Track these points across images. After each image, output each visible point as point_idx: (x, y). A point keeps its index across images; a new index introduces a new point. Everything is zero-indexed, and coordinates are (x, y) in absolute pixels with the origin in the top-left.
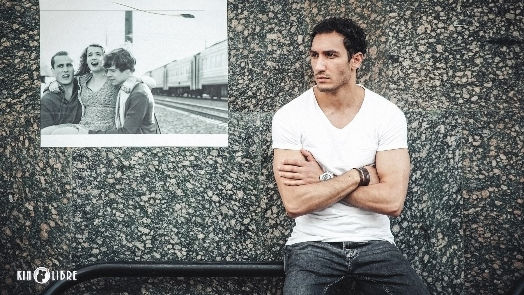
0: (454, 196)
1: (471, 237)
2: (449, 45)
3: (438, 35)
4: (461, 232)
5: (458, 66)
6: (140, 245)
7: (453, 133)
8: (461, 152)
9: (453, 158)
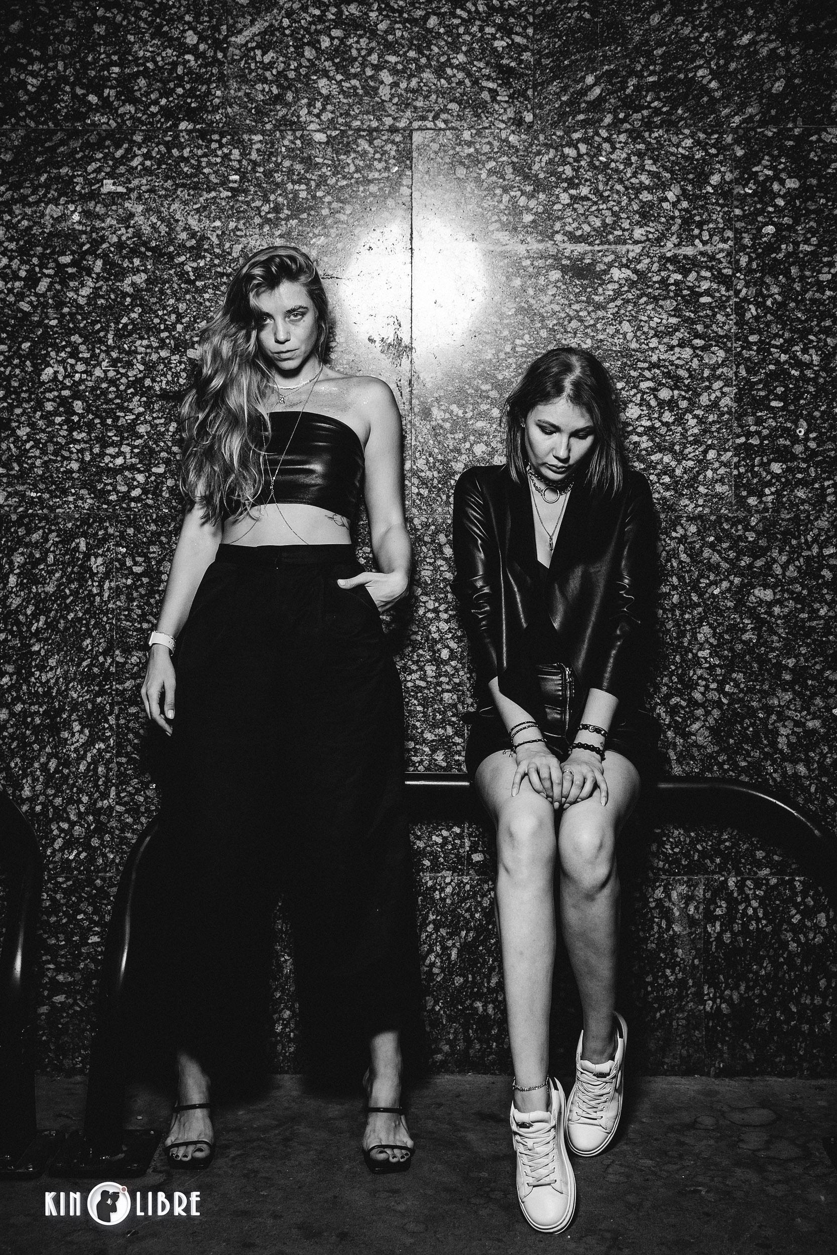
0: (101, 659)
1: (128, 728)
2: (94, 401)
3: (77, 384)
4: (112, 720)
5: (110, 437)
7: (100, 552)
8: (113, 584)
9: (100, 594)
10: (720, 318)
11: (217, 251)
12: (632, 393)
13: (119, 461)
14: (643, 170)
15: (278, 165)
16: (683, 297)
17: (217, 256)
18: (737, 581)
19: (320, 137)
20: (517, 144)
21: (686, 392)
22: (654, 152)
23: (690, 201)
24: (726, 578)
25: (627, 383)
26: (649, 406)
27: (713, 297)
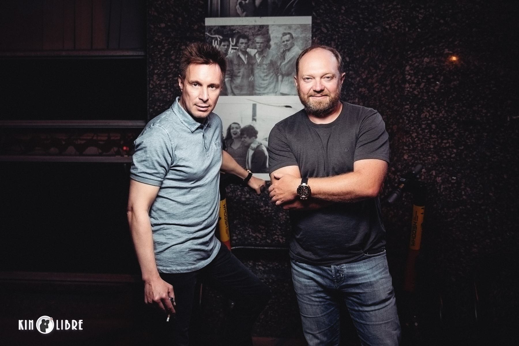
6: (260, 236)
9: (440, 190)
13: (448, 145)
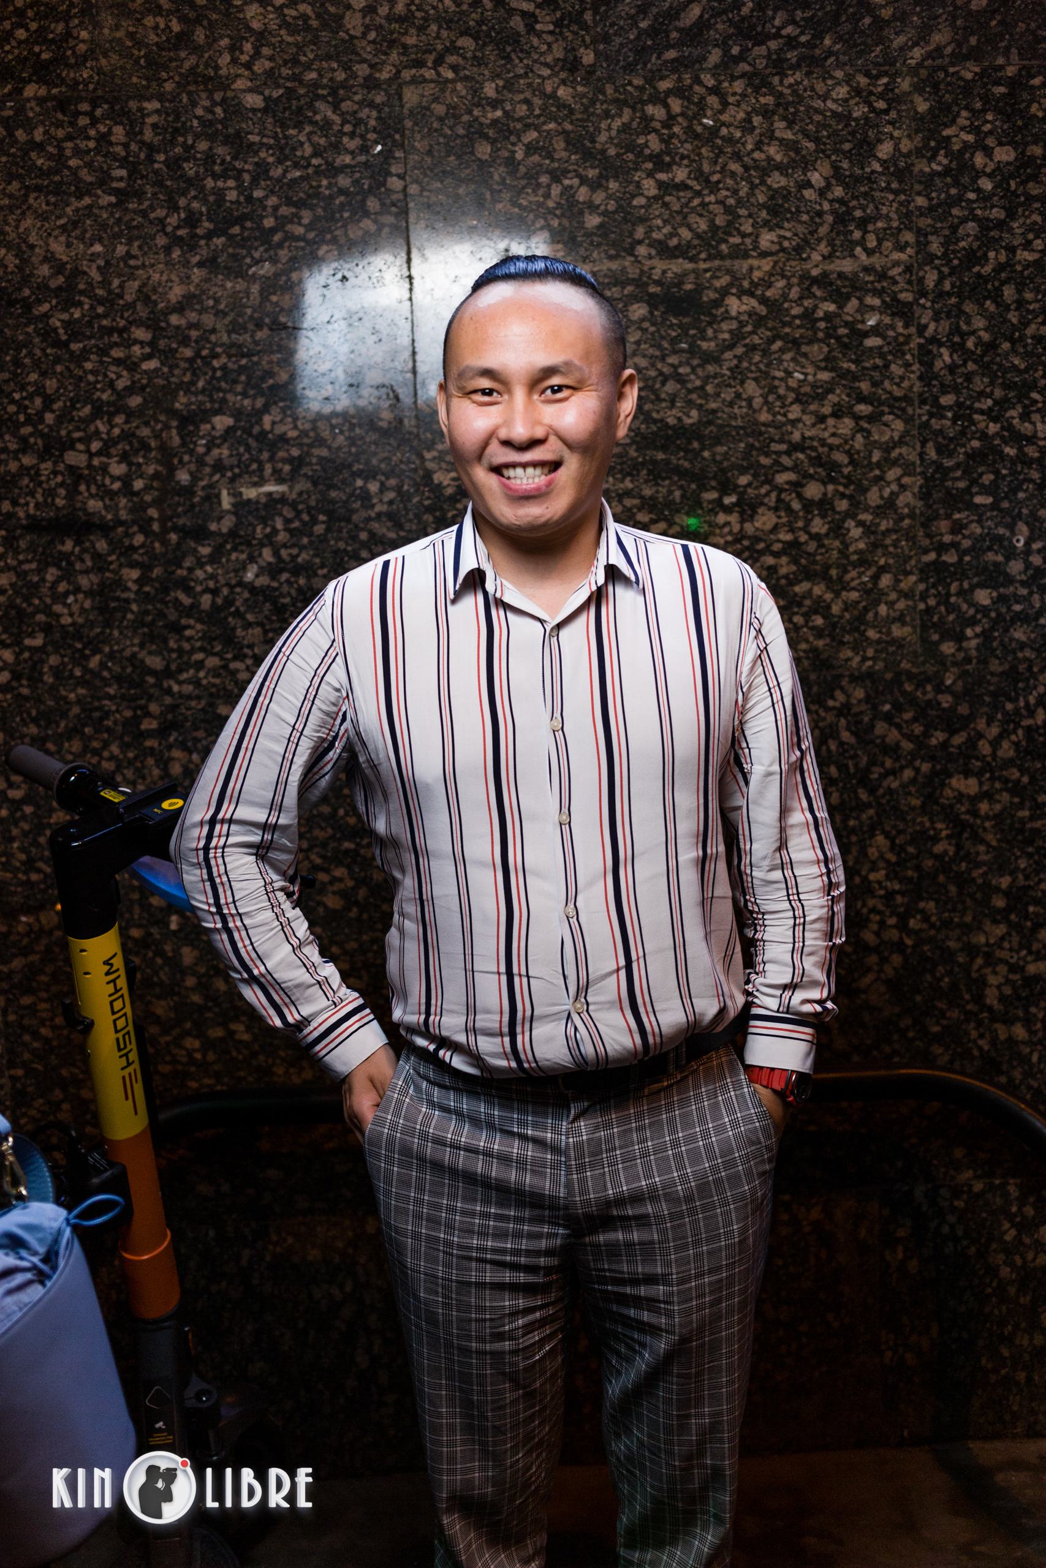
10: (896, 369)
11: (100, 292)
12: (763, 491)
14: (772, 137)
15: (188, 148)
16: (838, 338)
17: (101, 302)
18: (925, 767)
19: (253, 100)
20: (570, 101)
21: (846, 486)
22: (788, 108)
23: (846, 186)
24: (910, 764)
25: (755, 476)
26: (789, 509)
27: (884, 337)
